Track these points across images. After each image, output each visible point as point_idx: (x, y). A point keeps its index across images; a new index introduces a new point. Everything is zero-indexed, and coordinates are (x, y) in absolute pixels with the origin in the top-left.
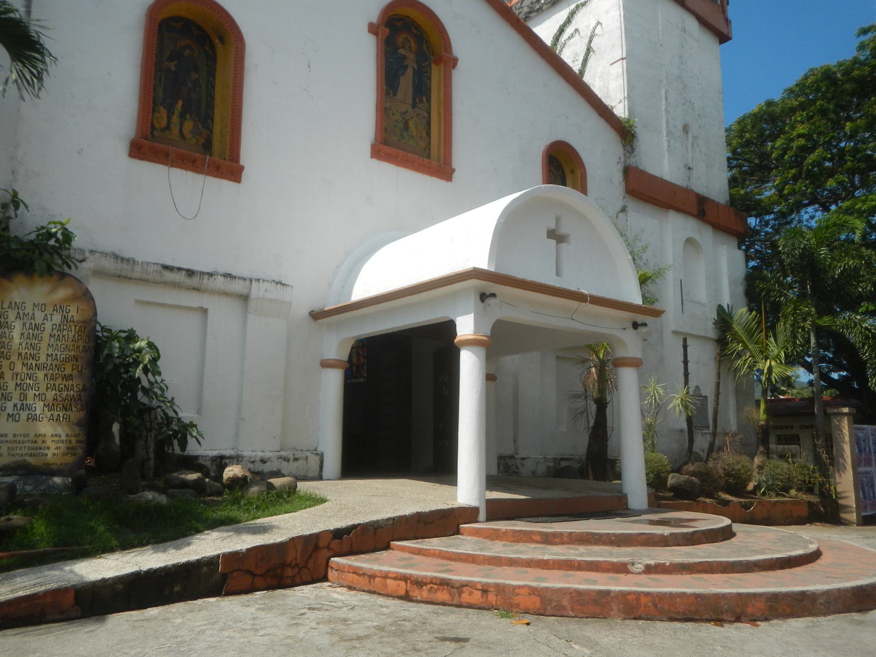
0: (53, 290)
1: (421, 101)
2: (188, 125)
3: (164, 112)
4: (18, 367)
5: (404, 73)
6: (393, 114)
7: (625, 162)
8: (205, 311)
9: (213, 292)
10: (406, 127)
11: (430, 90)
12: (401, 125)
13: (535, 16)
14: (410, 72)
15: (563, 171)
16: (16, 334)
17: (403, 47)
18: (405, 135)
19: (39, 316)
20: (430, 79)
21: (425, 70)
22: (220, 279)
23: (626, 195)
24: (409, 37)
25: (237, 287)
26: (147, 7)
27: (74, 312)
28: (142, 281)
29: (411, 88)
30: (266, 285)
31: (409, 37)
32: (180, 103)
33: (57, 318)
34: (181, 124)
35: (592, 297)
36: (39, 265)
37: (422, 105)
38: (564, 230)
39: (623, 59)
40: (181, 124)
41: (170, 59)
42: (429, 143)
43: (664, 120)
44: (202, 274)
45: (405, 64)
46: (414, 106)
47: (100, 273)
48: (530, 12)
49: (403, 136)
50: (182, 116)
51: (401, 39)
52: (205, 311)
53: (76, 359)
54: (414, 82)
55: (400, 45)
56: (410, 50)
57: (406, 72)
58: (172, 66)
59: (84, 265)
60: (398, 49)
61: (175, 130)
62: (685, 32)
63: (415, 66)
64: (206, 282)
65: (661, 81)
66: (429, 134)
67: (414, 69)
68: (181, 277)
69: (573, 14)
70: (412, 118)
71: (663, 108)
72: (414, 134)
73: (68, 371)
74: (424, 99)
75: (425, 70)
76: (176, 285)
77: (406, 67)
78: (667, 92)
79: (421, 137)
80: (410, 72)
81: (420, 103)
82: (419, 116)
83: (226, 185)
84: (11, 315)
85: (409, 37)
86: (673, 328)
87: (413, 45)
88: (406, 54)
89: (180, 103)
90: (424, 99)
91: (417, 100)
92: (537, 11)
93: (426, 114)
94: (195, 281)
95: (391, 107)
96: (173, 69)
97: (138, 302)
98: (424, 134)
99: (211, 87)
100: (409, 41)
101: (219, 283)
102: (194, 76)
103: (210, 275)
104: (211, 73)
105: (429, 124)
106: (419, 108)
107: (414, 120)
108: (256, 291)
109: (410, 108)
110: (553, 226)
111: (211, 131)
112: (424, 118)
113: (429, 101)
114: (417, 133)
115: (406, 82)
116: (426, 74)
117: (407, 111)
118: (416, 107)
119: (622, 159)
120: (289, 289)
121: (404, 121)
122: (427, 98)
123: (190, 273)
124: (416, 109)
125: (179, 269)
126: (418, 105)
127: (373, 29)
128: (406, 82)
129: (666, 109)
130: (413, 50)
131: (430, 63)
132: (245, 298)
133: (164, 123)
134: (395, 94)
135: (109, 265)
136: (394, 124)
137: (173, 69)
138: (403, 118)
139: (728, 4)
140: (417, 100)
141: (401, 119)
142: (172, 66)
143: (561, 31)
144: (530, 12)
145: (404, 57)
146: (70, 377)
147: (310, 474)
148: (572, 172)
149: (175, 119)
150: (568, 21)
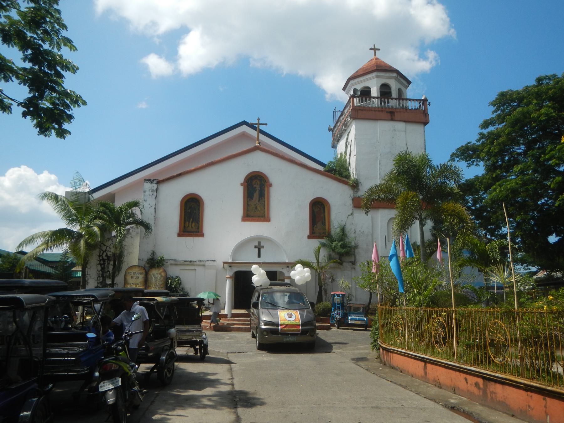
0: (159, 270)
1: (262, 199)
2: (193, 224)
3: (187, 223)
4: (154, 286)
7: (354, 196)
9: (197, 265)
10: (256, 208)
11: (265, 194)
14: (257, 192)
15: (324, 205)
16: (153, 280)
17: (255, 184)
19: (157, 276)
22: (198, 262)
23: (354, 208)
24: (257, 181)
25: (202, 263)
27: (163, 274)
28: (181, 265)
29: (258, 196)
30: (209, 262)
32: (191, 219)
33: (160, 276)
34: (192, 225)
35: (262, 263)
36: (156, 266)
38: (261, 245)
39: (355, 155)
40: (192, 225)
43: (379, 172)
44: (193, 261)
46: (259, 201)
47: (171, 264)
48: (341, 134)
50: (192, 222)
51: (254, 182)
52: (196, 270)
53: (163, 284)
54: (259, 194)
56: (257, 184)
59: (168, 263)
61: (190, 226)
62: (395, 130)
63: (260, 189)
64: (194, 263)
65: (377, 158)
66: (265, 208)
68: (188, 263)
69: (348, 135)
71: (379, 168)
72: (259, 209)
73: (162, 286)
74: (263, 198)
76: (188, 265)
77: (256, 190)
78: (380, 161)
80: (257, 192)
83: (201, 238)
84: (152, 276)
85: (257, 181)
87: (258, 182)
89: (191, 219)
90: (263, 198)
92: (343, 133)
93: (263, 202)
94: (192, 263)
97: (180, 269)
98: (263, 208)
100: (257, 182)
101: (198, 263)
103: (195, 261)
104: (199, 210)
105: (265, 205)
108: (207, 263)
109: (257, 202)
110: (257, 244)
111: (199, 224)
113: (265, 198)
115: (256, 195)
119: (352, 195)
120: (215, 262)
123: (191, 262)
125: (188, 261)
127: (242, 184)
129: (379, 168)
131: (265, 187)
132: (204, 265)
133: (188, 225)
135: (173, 262)
139: (430, 106)
142: (189, 211)
143: (347, 142)
144: (341, 134)
146: (162, 288)
147: (222, 308)
148: (326, 205)
149: (190, 224)
150: (347, 138)
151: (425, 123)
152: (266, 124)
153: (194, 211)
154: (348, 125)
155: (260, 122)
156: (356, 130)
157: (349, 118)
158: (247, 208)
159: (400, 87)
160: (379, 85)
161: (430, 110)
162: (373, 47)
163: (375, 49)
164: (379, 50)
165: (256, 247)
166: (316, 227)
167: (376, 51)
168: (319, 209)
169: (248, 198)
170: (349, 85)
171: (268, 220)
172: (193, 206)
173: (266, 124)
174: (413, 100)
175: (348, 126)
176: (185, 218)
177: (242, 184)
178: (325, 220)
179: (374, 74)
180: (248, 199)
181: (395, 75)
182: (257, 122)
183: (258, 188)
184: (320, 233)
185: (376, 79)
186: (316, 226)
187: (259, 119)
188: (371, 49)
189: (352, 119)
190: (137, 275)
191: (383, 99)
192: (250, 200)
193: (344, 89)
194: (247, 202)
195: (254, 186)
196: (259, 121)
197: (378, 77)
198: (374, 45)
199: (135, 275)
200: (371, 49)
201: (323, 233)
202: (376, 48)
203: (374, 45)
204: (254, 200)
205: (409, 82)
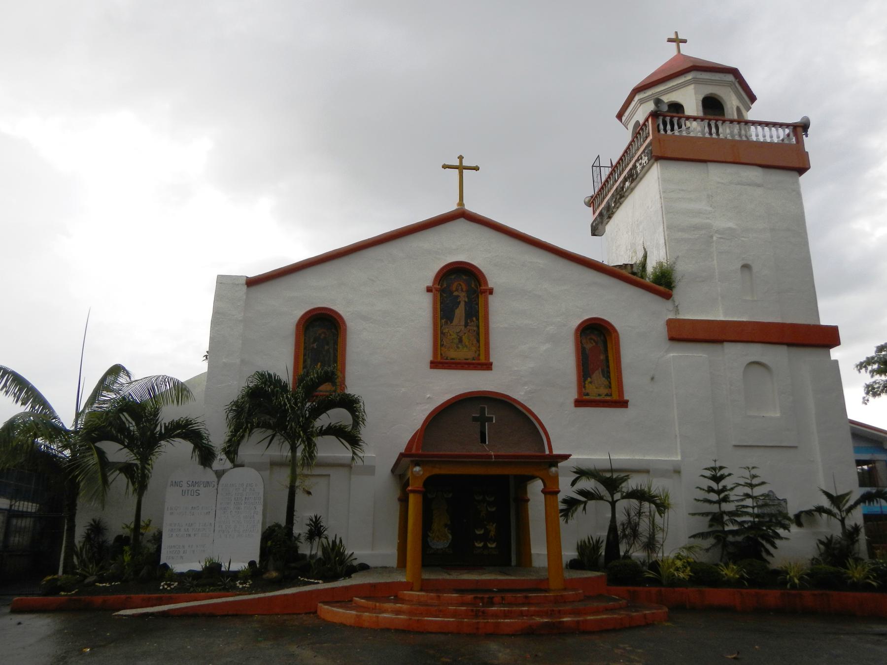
5: (458, 307)
6: (450, 335)
8: (329, 475)
10: (461, 340)
12: (456, 341)
13: (625, 199)
14: (462, 305)
17: (457, 290)
18: (460, 346)
20: (478, 304)
21: (474, 300)
26: (296, 322)
31: (462, 284)
37: (473, 323)
41: (314, 343)
42: (479, 347)
45: (458, 300)
46: (466, 325)
49: (458, 348)
51: (454, 287)
52: (329, 475)
54: (465, 309)
55: (454, 289)
56: (462, 290)
57: (460, 306)
58: (315, 346)
60: (453, 293)
63: (467, 300)
66: (478, 341)
67: (465, 302)
70: (465, 334)
72: (467, 344)
75: (474, 300)
77: (460, 302)
79: (472, 344)
81: (471, 322)
82: (471, 331)
85: (462, 284)
86: (734, 443)
88: (460, 294)
90: (474, 319)
91: (469, 321)
93: (475, 328)
95: (448, 331)
96: (315, 347)
98: (475, 342)
99: (336, 350)
100: (460, 285)
102: (326, 347)
104: (336, 343)
105: (478, 334)
106: (470, 326)
107: (466, 335)
112: (474, 331)
113: (478, 319)
114: (469, 342)
115: (460, 312)
116: (475, 302)
117: (461, 331)
118: (468, 325)
121: (459, 337)
122: (476, 318)
124: (468, 327)
126: (470, 324)
128: (460, 312)
130: (464, 290)
134: (451, 322)
136: (451, 341)
137: (315, 347)
138: (458, 336)
139: (807, 136)
140: (469, 321)
141: (456, 336)
142: (315, 346)
145: (458, 296)
151: (802, 169)
152: (476, 169)
153: (326, 347)
154: (640, 176)
155: (464, 165)
156: (664, 180)
157: (645, 159)
158: (442, 341)
159: (739, 106)
160: (701, 97)
161: (810, 143)
162: (673, 36)
163: (677, 40)
164: (685, 41)
165: (475, 419)
166: (591, 383)
167: (681, 44)
168: (594, 344)
169: (441, 319)
170: (633, 104)
171: (487, 366)
172: (323, 335)
173: (476, 169)
174: (775, 125)
175: (641, 179)
176: (305, 361)
177: (429, 290)
178: (608, 367)
179: (689, 76)
180: (443, 321)
181: (730, 78)
182: (457, 163)
183: (463, 297)
184: (599, 395)
185: (692, 86)
186: (589, 379)
187: (461, 158)
188: (670, 40)
189: (652, 161)
190: (196, 488)
191: (713, 123)
192: (446, 323)
193: (620, 116)
194: (441, 327)
195: (456, 293)
196: (461, 162)
197: (695, 81)
198: (676, 33)
199: (191, 488)
200: (670, 40)
201: (607, 395)
202: (680, 38)
203: (676, 33)
204: (455, 321)
205: (753, 98)
